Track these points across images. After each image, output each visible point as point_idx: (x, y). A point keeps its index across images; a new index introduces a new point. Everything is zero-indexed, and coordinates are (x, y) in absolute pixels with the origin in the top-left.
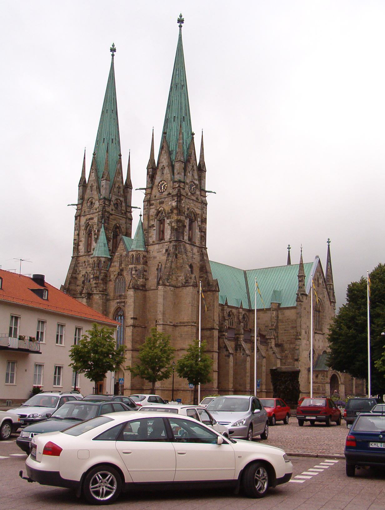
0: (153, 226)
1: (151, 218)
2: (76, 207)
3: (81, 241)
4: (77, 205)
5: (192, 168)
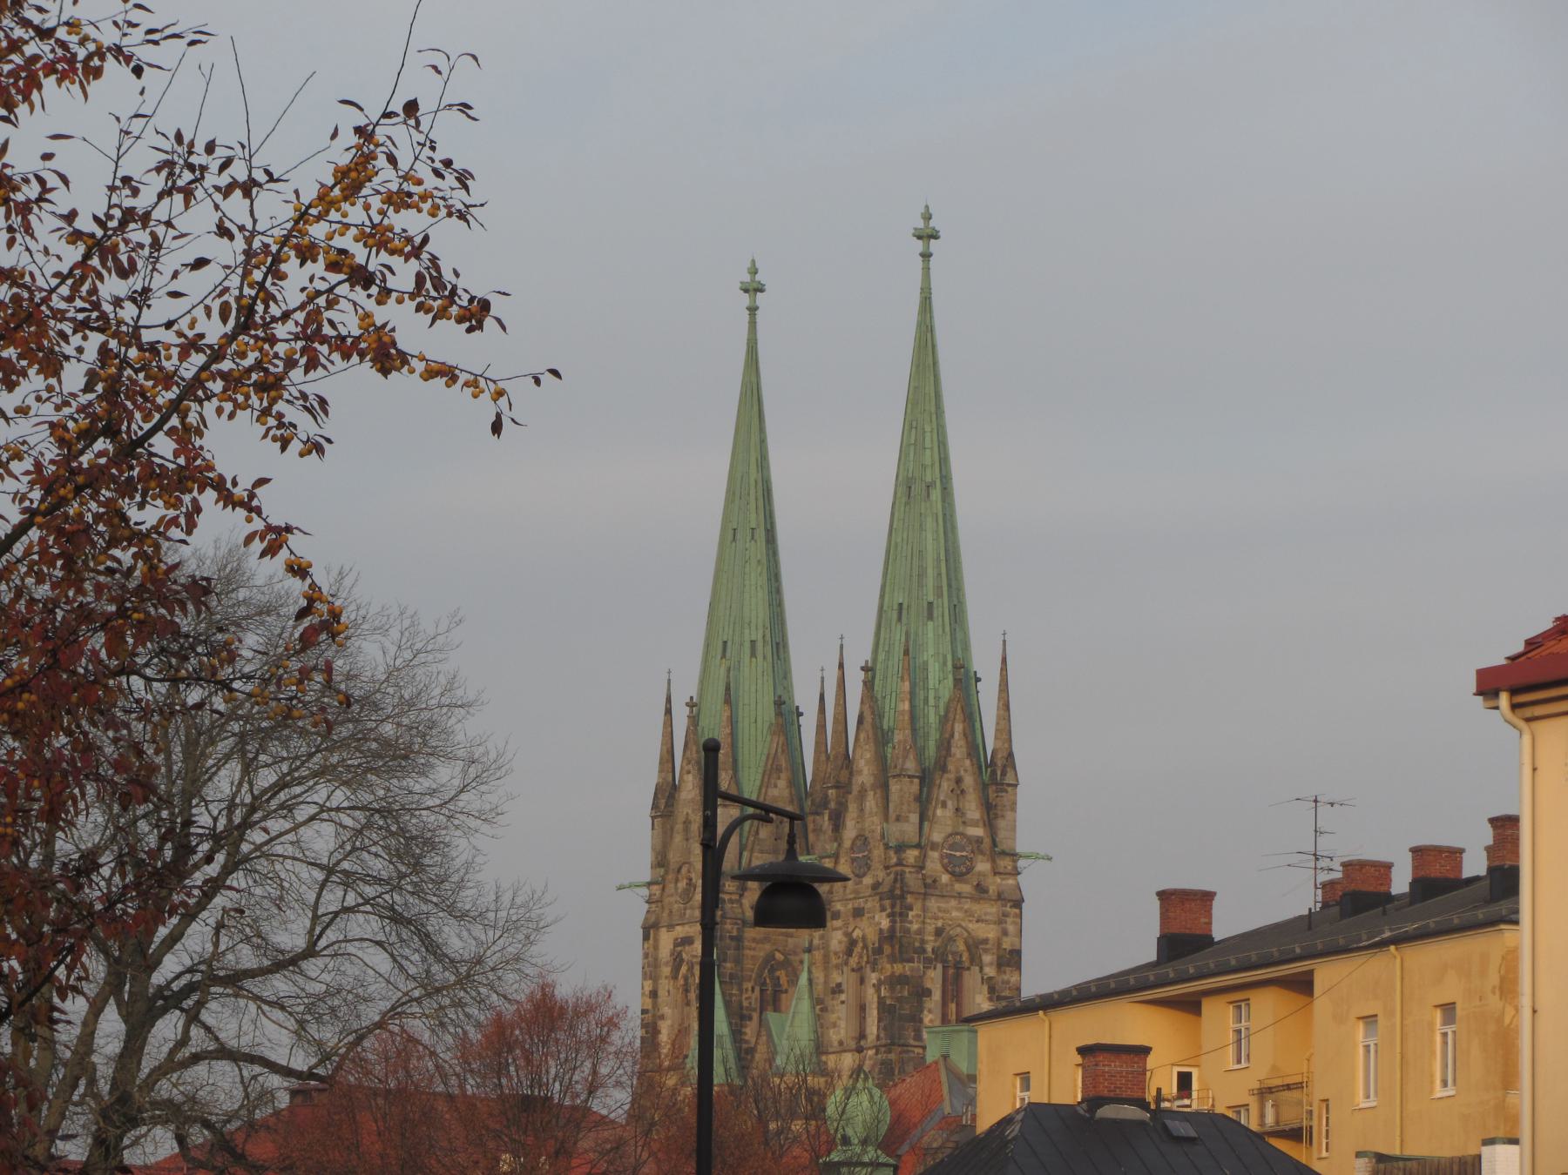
0: (838, 989)
1: (834, 961)
2: (645, 892)
3: (662, 1017)
4: (649, 885)
5: (953, 785)
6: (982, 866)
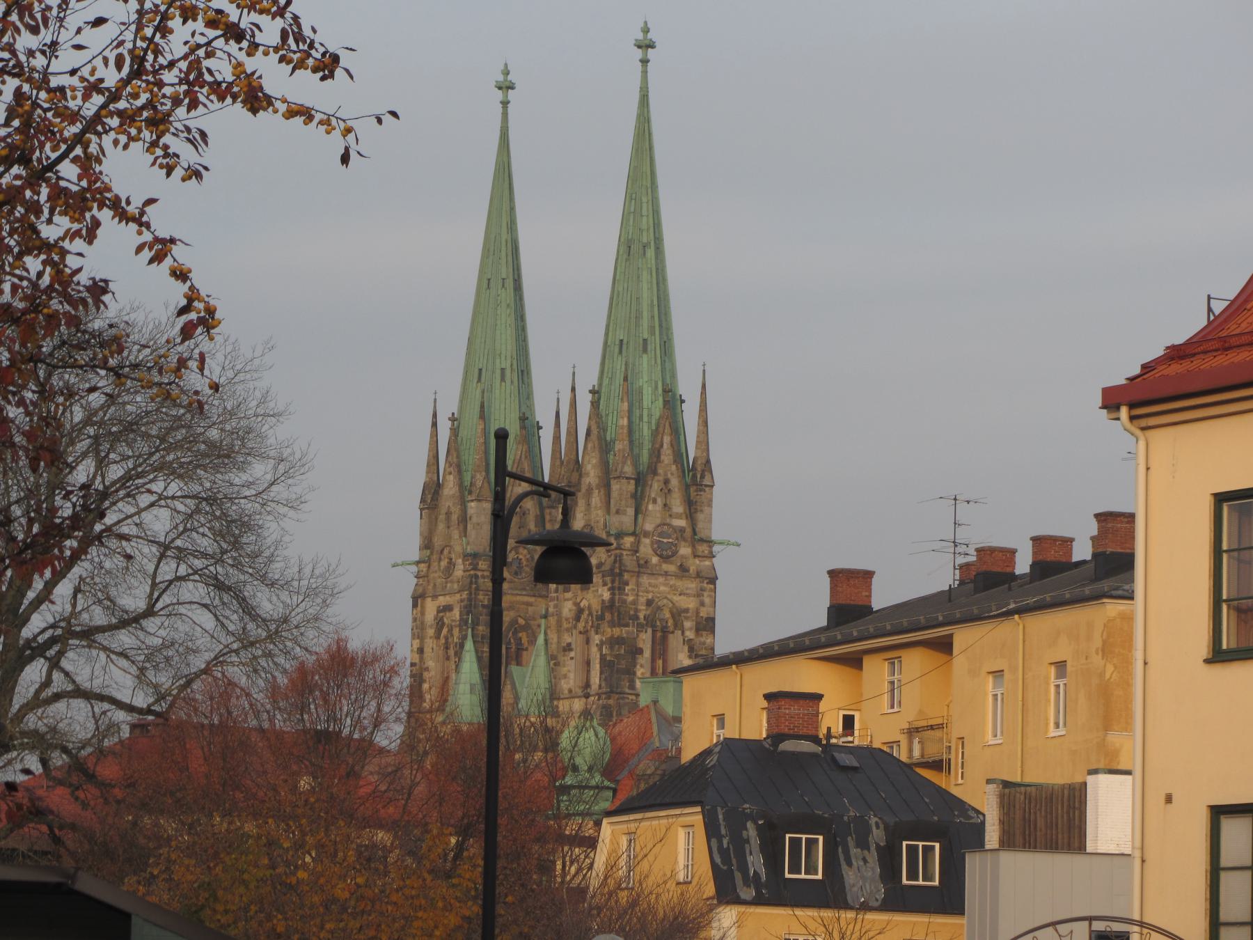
0: (568, 648)
1: (565, 625)
2: (414, 569)
4: (418, 563)
5: (662, 486)
6: (685, 550)
